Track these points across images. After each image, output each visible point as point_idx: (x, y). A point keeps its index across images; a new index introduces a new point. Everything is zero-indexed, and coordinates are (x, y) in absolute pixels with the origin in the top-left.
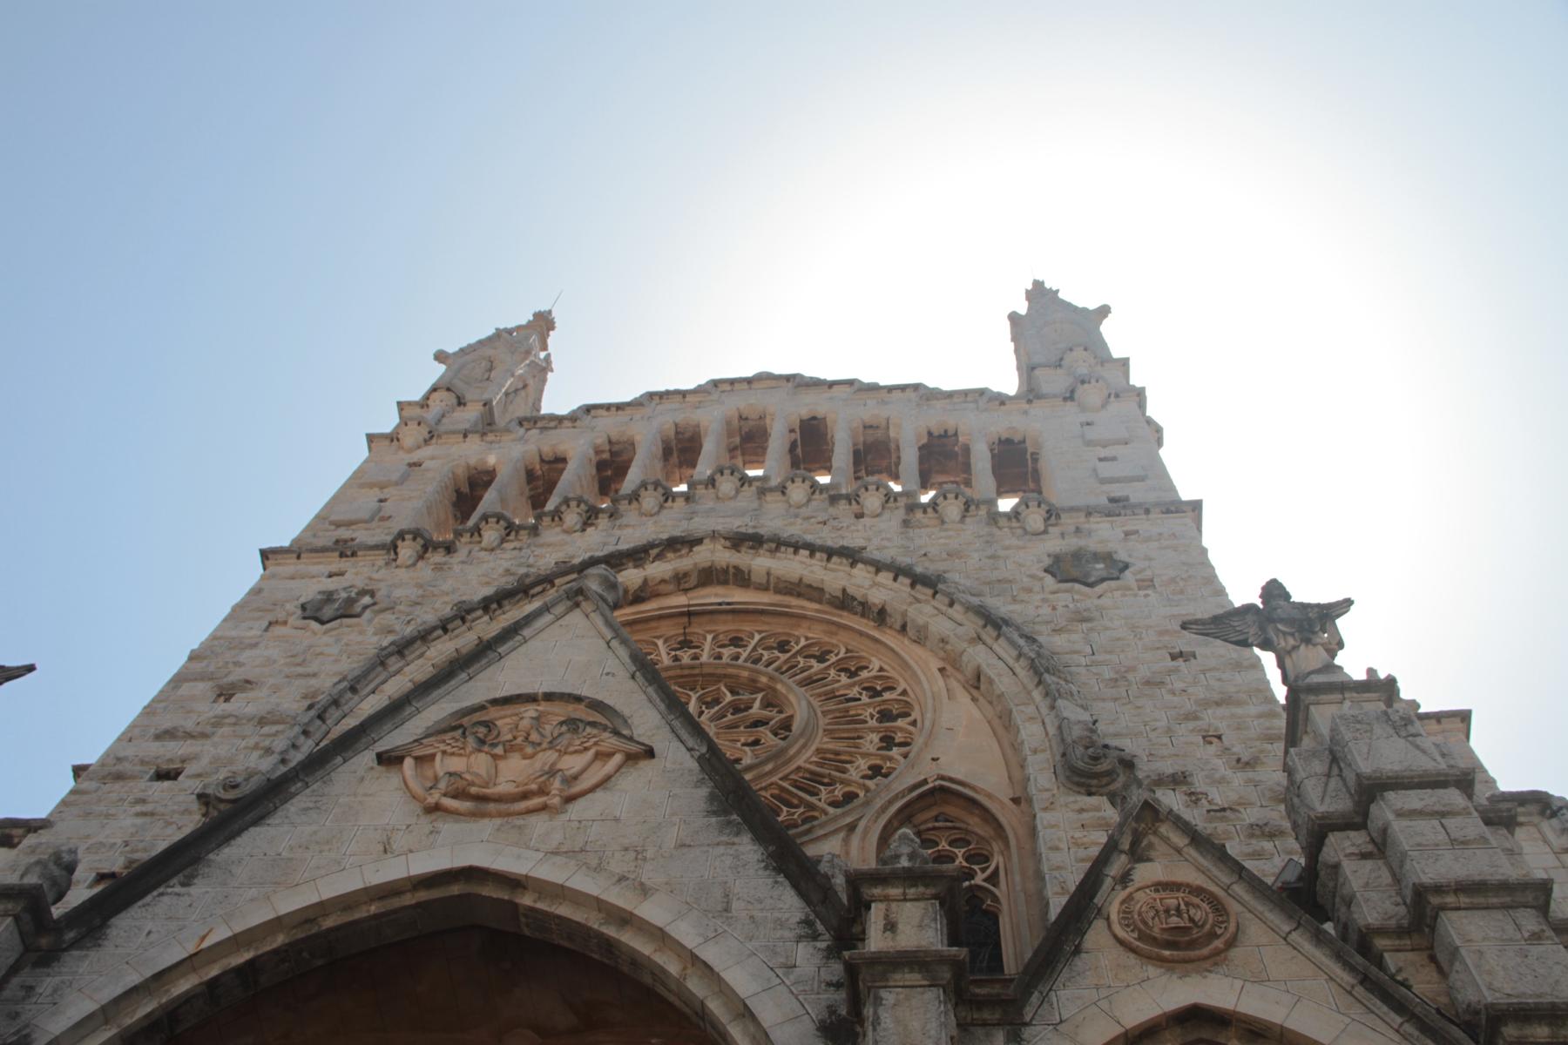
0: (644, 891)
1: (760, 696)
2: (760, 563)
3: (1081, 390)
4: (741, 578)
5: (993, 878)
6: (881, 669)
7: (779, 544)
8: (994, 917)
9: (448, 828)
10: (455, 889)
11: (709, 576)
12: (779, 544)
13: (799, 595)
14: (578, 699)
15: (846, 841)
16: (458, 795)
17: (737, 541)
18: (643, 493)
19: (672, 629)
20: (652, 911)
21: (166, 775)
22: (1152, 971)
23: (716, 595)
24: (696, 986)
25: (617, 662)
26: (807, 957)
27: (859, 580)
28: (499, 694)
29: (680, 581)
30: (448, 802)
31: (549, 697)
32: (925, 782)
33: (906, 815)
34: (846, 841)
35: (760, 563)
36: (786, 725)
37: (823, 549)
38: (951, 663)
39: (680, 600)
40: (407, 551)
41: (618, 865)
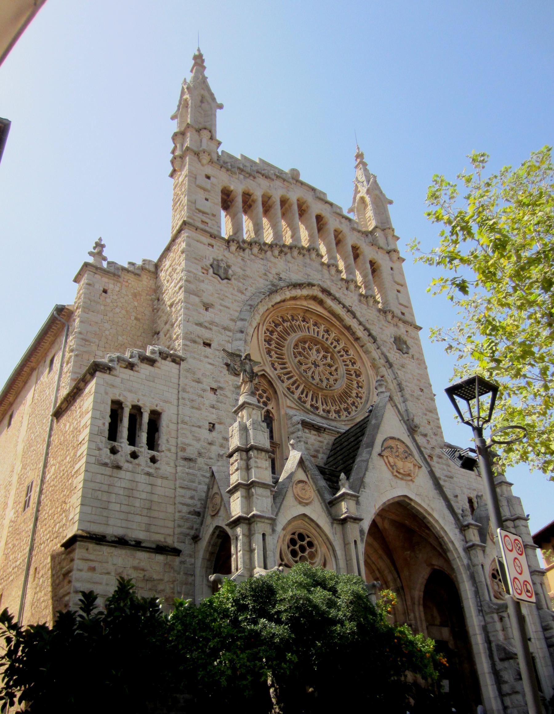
1: (329, 355)
2: (329, 302)
3: (393, 252)
4: (321, 302)
7: (335, 299)
9: (399, 482)
11: (315, 298)
12: (335, 299)
13: (335, 317)
16: (397, 472)
17: (324, 291)
18: (294, 249)
20: (435, 515)
24: (442, 533)
26: (457, 531)
29: (307, 298)
31: (398, 439)
35: (329, 302)
37: (347, 308)
38: (374, 366)
39: (305, 303)
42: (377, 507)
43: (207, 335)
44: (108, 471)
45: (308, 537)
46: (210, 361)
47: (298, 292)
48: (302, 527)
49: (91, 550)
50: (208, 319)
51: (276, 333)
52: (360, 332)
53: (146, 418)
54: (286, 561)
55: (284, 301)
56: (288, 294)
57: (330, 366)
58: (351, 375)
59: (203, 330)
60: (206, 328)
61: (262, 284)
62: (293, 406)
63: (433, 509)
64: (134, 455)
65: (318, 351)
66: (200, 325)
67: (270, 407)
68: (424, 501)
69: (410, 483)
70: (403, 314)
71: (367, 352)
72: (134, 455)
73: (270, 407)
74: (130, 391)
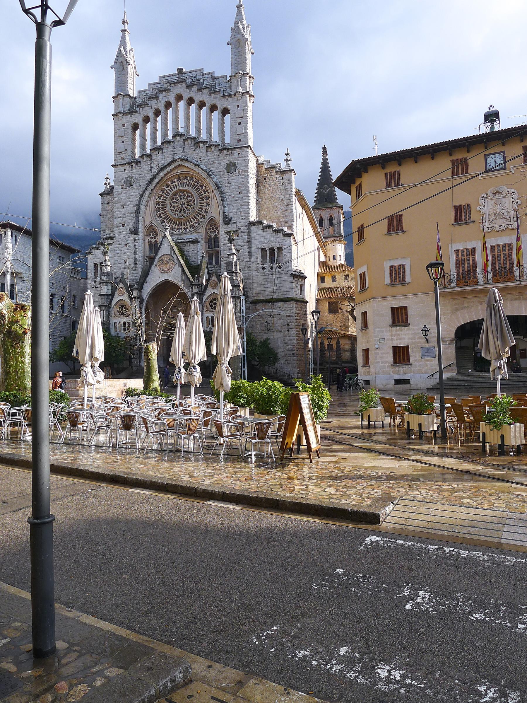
2: (186, 164)
5: (218, 233)
11: (179, 165)
16: (163, 270)
17: (182, 160)
19: (177, 177)
21: (123, 225)
29: (176, 168)
39: (176, 171)
40: (134, 166)
43: (122, 220)
47: (168, 169)
50: (123, 212)
55: (162, 178)
56: (162, 174)
57: (191, 201)
61: (149, 177)
65: (184, 195)
66: (120, 217)
70: (239, 141)
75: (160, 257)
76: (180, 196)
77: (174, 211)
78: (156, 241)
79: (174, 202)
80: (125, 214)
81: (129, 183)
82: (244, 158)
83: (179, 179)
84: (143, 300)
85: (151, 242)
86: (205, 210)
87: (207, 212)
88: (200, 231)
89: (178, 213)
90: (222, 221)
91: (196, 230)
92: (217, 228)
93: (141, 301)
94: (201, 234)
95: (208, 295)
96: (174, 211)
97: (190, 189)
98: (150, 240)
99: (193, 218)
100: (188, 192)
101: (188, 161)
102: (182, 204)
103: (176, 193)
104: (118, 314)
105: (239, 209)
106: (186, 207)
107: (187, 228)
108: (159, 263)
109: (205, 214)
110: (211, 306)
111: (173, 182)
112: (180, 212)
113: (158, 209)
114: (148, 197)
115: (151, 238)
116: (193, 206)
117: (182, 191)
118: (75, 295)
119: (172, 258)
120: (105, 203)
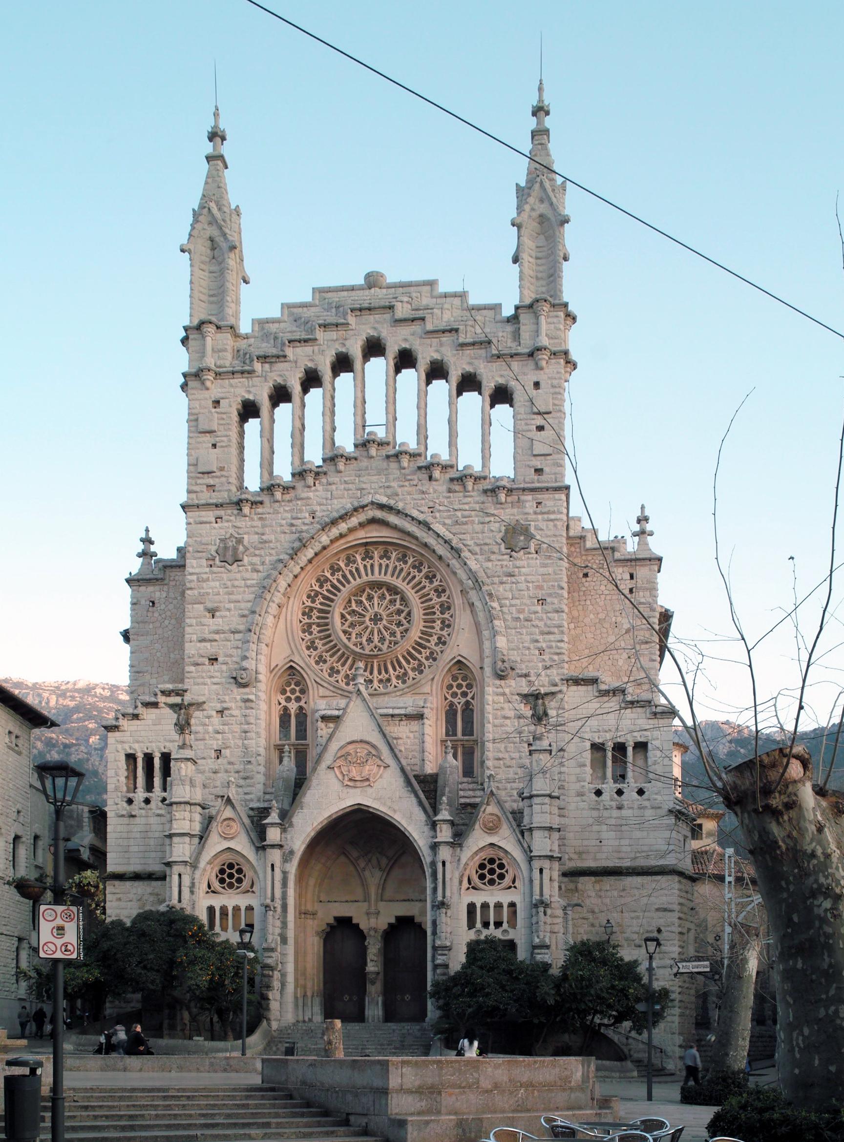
0: (395, 811)
1: (398, 597)
6: (441, 581)
8: (472, 710)
9: (352, 791)
10: (356, 807)
14: (368, 743)
15: (432, 686)
16: (350, 780)
21: (213, 660)
22: (486, 835)
23: (376, 530)
25: (373, 726)
26: (426, 829)
27: (431, 541)
28: (348, 740)
30: (349, 783)
31: (361, 741)
32: (455, 658)
33: (450, 669)
34: (432, 686)
36: (409, 614)
41: (389, 804)
42: (315, 824)
44: (126, 820)
45: (238, 864)
46: (215, 680)
48: (229, 858)
49: (117, 886)
51: (320, 596)
52: (441, 550)
53: (157, 762)
54: (212, 889)
57: (399, 612)
58: (434, 613)
59: (208, 645)
60: (211, 641)
62: (328, 693)
63: (395, 811)
64: (147, 801)
65: (383, 597)
66: (203, 640)
67: (302, 703)
68: (385, 804)
69: (368, 789)
71: (455, 573)
72: (147, 801)
73: (302, 703)
74: (138, 742)
75: (342, 748)
76: (370, 598)
77: (354, 635)
78: (301, 708)
79: (353, 612)
80: (217, 632)
81: (229, 555)
82: (552, 517)
83: (367, 556)
84: (292, 852)
85: (286, 709)
86: (439, 638)
87: (444, 643)
88: (427, 689)
89: (364, 639)
90: (488, 671)
91: (414, 689)
92: (470, 686)
93: (287, 857)
94: (431, 696)
95: (475, 849)
96: (354, 635)
97: (399, 583)
98: (284, 703)
99: (404, 657)
100: (393, 590)
101: (399, 512)
102: (376, 619)
103: (361, 590)
104: (216, 885)
105: (537, 641)
106: (386, 628)
107: (389, 680)
108: (340, 762)
109: (437, 649)
110: (482, 877)
111: (350, 560)
112: (370, 640)
113: (307, 629)
114: (284, 595)
115: (288, 700)
116: (406, 625)
117: (377, 585)
118: (38, 834)
119: (374, 752)
120: (143, 602)
